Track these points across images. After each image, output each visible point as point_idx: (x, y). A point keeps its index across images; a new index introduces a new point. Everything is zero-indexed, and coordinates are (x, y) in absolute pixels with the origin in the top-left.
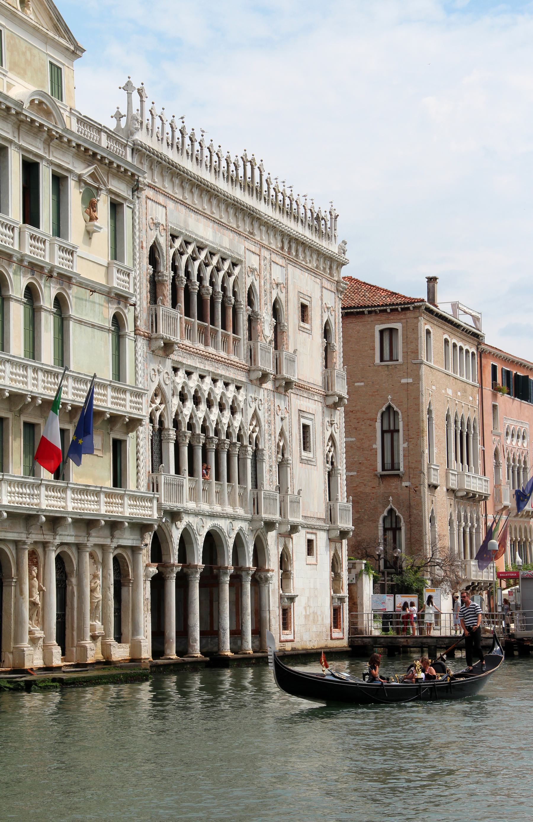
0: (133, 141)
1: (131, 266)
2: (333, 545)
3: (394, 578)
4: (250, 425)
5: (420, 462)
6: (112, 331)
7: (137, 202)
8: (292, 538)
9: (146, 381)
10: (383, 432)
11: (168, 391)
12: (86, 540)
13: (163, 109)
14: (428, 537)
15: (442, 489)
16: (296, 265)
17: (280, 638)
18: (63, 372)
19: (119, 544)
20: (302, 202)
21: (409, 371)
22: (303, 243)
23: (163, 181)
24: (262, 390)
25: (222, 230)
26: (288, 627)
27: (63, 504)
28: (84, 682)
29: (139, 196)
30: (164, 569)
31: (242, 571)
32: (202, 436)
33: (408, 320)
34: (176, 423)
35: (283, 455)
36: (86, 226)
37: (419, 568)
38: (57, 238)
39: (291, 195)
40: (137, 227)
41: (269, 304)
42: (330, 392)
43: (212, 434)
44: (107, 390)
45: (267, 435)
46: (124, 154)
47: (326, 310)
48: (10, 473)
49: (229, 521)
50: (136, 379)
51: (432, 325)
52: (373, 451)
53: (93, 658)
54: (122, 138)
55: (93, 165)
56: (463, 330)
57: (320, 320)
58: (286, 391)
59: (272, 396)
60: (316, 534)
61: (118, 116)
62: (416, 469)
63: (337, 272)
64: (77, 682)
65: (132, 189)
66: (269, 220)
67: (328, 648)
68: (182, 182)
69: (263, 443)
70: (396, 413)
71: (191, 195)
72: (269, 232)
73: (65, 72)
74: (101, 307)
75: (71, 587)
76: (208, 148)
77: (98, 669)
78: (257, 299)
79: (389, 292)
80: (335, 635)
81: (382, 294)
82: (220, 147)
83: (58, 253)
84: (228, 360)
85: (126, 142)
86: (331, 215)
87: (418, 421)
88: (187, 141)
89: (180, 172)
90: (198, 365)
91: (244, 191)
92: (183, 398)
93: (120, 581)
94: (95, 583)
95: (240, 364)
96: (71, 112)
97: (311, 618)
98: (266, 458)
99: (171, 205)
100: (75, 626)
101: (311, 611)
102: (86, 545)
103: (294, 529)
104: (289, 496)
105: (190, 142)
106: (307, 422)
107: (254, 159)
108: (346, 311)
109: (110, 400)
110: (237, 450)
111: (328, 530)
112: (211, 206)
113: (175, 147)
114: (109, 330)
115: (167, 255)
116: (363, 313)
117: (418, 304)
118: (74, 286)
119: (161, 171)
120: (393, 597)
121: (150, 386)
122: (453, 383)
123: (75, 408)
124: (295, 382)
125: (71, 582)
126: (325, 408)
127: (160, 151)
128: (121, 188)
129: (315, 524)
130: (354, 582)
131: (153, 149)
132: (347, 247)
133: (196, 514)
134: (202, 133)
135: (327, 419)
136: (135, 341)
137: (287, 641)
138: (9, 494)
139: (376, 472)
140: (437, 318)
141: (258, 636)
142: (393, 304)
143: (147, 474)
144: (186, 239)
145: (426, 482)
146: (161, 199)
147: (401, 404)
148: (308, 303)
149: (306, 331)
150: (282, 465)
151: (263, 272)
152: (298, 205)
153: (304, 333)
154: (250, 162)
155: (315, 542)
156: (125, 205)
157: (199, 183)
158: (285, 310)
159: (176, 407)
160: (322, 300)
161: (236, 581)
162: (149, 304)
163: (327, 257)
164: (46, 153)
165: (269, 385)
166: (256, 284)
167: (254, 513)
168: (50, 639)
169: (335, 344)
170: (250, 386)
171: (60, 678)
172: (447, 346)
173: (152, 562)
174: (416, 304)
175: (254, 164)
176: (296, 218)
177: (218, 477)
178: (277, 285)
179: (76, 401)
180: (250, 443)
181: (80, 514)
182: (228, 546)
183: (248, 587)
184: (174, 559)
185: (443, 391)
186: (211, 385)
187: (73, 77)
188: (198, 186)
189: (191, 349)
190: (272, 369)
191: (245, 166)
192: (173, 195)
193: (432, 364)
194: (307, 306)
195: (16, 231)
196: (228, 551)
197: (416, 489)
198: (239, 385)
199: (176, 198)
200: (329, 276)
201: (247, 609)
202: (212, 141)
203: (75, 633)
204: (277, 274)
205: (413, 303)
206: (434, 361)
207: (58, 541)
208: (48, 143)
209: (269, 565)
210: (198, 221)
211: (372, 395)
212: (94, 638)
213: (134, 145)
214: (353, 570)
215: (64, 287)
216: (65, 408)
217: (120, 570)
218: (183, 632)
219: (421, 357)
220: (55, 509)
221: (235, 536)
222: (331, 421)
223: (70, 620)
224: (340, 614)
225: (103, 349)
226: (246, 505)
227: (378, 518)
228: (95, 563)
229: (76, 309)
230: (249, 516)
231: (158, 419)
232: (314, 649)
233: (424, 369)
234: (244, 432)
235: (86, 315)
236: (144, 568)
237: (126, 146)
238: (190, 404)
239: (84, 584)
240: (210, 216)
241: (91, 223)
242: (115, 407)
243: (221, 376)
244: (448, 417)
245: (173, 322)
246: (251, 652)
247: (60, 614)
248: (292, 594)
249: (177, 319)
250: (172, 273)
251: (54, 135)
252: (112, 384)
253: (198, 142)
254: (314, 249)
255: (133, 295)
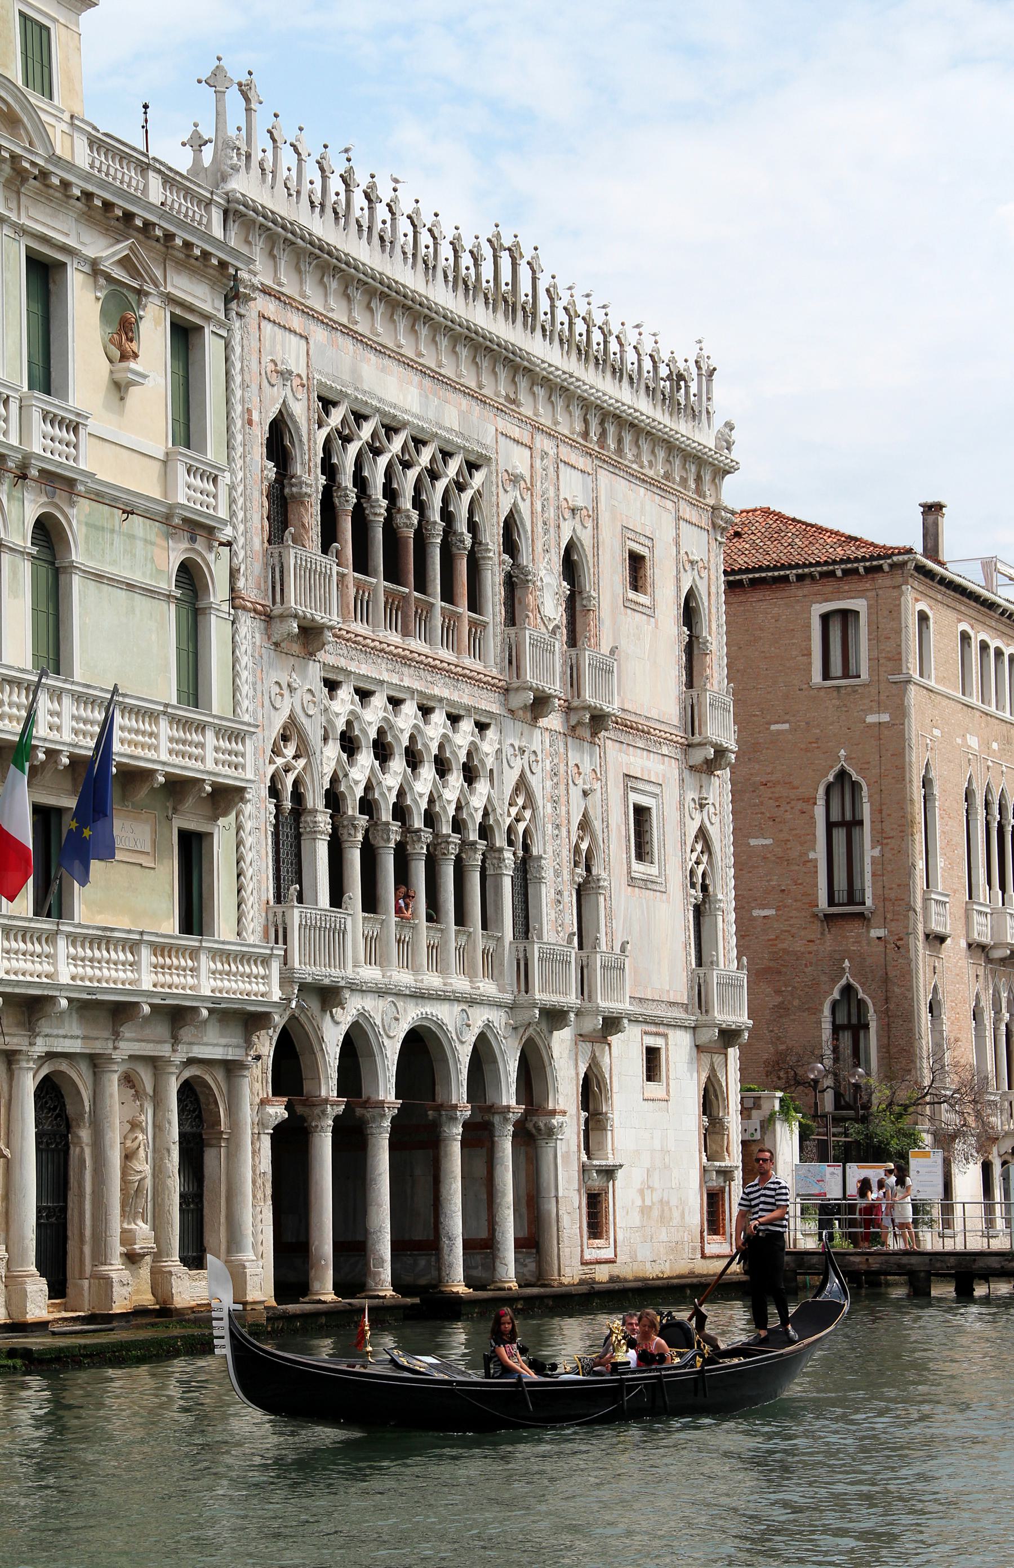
0: (227, 194)
1: (223, 462)
2: (706, 1058)
3: (855, 1129)
4: (510, 805)
5: (906, 886)
6: (177, 599)
7: (237, 324)
8: (609, 1044)
9: (260, 709)
10: (830, 826)
11: (314, 732)
12: (111, 1046)
13: (301, 129)
14: (926, 1042)
15: (958, 944)
16: (617, 471)
17: (582, 1257)
18: (36, 679)
19: (190, 1055)
20: (631, 337)
21: (883, 697)
22: (632, 425)
23: (301, 282)
24: (537, 732)
25: (441, 393)
26: (601, 1233)
27: (48, 968)
28: (85, 1356)
29: (242, 311)
30: (307, 1109)
31: (494, 1113)
32: (395, 826)
33: (880, 592)
34: (334, 799)
35: (588, 869)
36: (111, 372)
37: (906, 1107)
38: (183, 450)
39: (606, 323)
40: (238, 379)
41: (553, 551)
42: (697, 738)
43: (418, 823)
44: (157, 724)
45: (550, 826)
46: (205, 221)
47: (688, 567)
48: (76, 921)
49: (460, 1008)
50: (236, 704)
51: (933, 603)
52: (809, 864)
53: (127, 1302)
54: (199, 186)
55: (128, 239)
56: (1002, 614)
57: (673, 588)
58: (594, 734)
59: (561, 745)
60: (665, 1036)
61: (197, 143)
62: (898, 904)
63: (713, 488)
64: (66, 1356)
65: (226, 296)
66: (551, 373)
67: (697, 1277)
68: (347, 287)
69: (541, 844)
70: (855, 786)
71: (368, 314)
72: (553, 399)
73: (58, 36)
74: (149, 547)
75: (78, 1149)
76: (409, 217)
77: (138, 1327)
78: (527, 539)
79: (842, 535)
80: (709, 1250)
81: (829, 541)
82: (436, 215)
83: (38, 426)
84: (456, 666)
85: (209, 196)
86: (699, 368)
87: (903, 802)
88: (359, 200)
89: (339, 264)
90: (385, 676)
91: (494, 311)
92: (349, 744)
93: (201, 1135)
94: (133, 1141)
95: (485, 675)
96: (72, 124)
97: (656, 1213)
98: (548, 874)
99: (319, 334)
100: (88, 1233)
101: (656, 1198)
102: (110, 1059)
103: (612, 1024)
104: (598, 956)
105: (365, 204)
106: (644, 801)
107: (517, 245)
108: (751, 576)
109: (164, 745)
110: (479, 857)
111: (694, 1028)
112: (417, 339)
113: (329, 211)
114: (169, 596)
115: (309, 440)
116: (785, 579)
117: (901, 558)
118: (82, 500)
119: (295, 261)
120: (841, 1168)
121: (269, 718)
122: (980, 724)
123: (75, 761)
124: (614, 715)
125: (79, 1137)
126: (686, 773)
127: (292, 218)
128: (200, 295)
129: (663, 1014)
130: (758, 1136)
131: (272, 212)
132: (735, 435)
133: (381, 992)
134: (394, 185)
135: (691, 795)
136: (233, 623)
137: (599, 1262)
138: (5, 955)
139: (815, 909)
140: (943, 588)
141: (534, 1251)
142: (849, 560)
143: (264, 906)
144: (356, 408)
145: (920, 927)
146: (296, 321)
147: (866, 766)
148: (647, 550)
149: (640, 609)
150: (585, 891)
151: (539, 484)
152: (621, 345)
153: (637, 614)
154: (509, 249)
155: (663, 1052)
156: (206, 331)
157: (386, 289)
158: (591, 565)
159: (333, 764)
160: (677, 544)
161: (479, 1136)
162: (266, 544)
163: (690, 455)
164: (10, 210)
165: (553, 721)
166: (524, 508)
167: (519, 991)
168: (23, 1262)
169: (709, 638)
170: (509, 723)
171: (25, 1349)
172: (966, 646)
173: (274, 1095)
174: (895, 558)
175: (517, 256)
176: (617, 372)
177: (434, 914)
178: (573, 511)
179: (81, 747)
180: (511, 843)
181: (164, 996)
182: (457, 1061)
183: (506, 1147)
184: (329, 1087)
185: (959, 741)
186: (415, 718)
187: (79, 49)
188: (383, 296)
189: (369, 641)
190: (557, 688)
191: (496, 258)
192: (324, 312)
193: (932, 683)
194: (642, 558)
195: (14, 406)
196: (458, 1072)
197: (899, 943)
198: (483, 720)
199: (331, 320)
200: (695, 496)
201: (504, 1195)
202: (417, 201)
203: (87, 1249)
204: (573, 487)
205: (890, 556)
206: (936, 677)
207: (40, 1047)
208: (14, 188)
209: (556, 1101)
210: (383, 370)
211: (807, 750)
212: (132, 1258)
213: (228, 202)
214: (754, 1112)
215: (56, 500)
216: (56, 762)
217: (200, 1112)
218: (352, 1247)
219: (908, 668)
220: (29, 979)
221: (474, 1039)
222: (701, 799)
223: (76, 1219)
224: (723, 1205)
225: (154, 637)
226: (501, 973)
227: (822, 1004)
228: (137, 1096)
229: (87, 550)
230: (508, 997)
231: (290, 789)
232: (662, 1279)
233: (913, 693)
234: (497, 821)
235: (114, 563)
236: (255, 1108)
237: (209, 203)
238: (366, 758)
239: (107, 1143)
240: (412, 360)
241: (124, 364)
242: (178, 760)
243: (441, 700)
244: (969, 795)
245: (321, 582)
246: (514, 1285)
247: (54, 1208)
248: (610, 1162)
249: (331, 576)
250: (322, 480)
251: (26, 170)
252: (169, 710)
253: (384, 203)
254: (659, 438)
255: (224, 522)
